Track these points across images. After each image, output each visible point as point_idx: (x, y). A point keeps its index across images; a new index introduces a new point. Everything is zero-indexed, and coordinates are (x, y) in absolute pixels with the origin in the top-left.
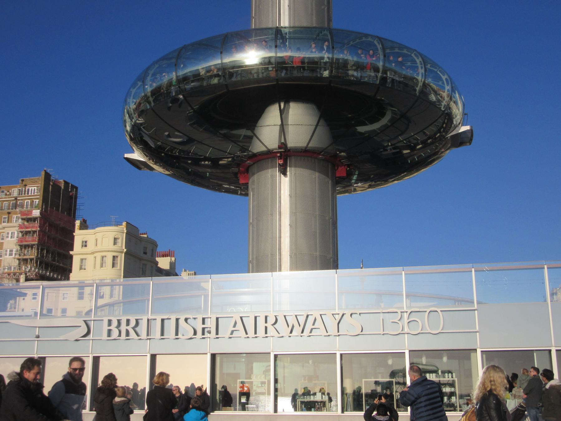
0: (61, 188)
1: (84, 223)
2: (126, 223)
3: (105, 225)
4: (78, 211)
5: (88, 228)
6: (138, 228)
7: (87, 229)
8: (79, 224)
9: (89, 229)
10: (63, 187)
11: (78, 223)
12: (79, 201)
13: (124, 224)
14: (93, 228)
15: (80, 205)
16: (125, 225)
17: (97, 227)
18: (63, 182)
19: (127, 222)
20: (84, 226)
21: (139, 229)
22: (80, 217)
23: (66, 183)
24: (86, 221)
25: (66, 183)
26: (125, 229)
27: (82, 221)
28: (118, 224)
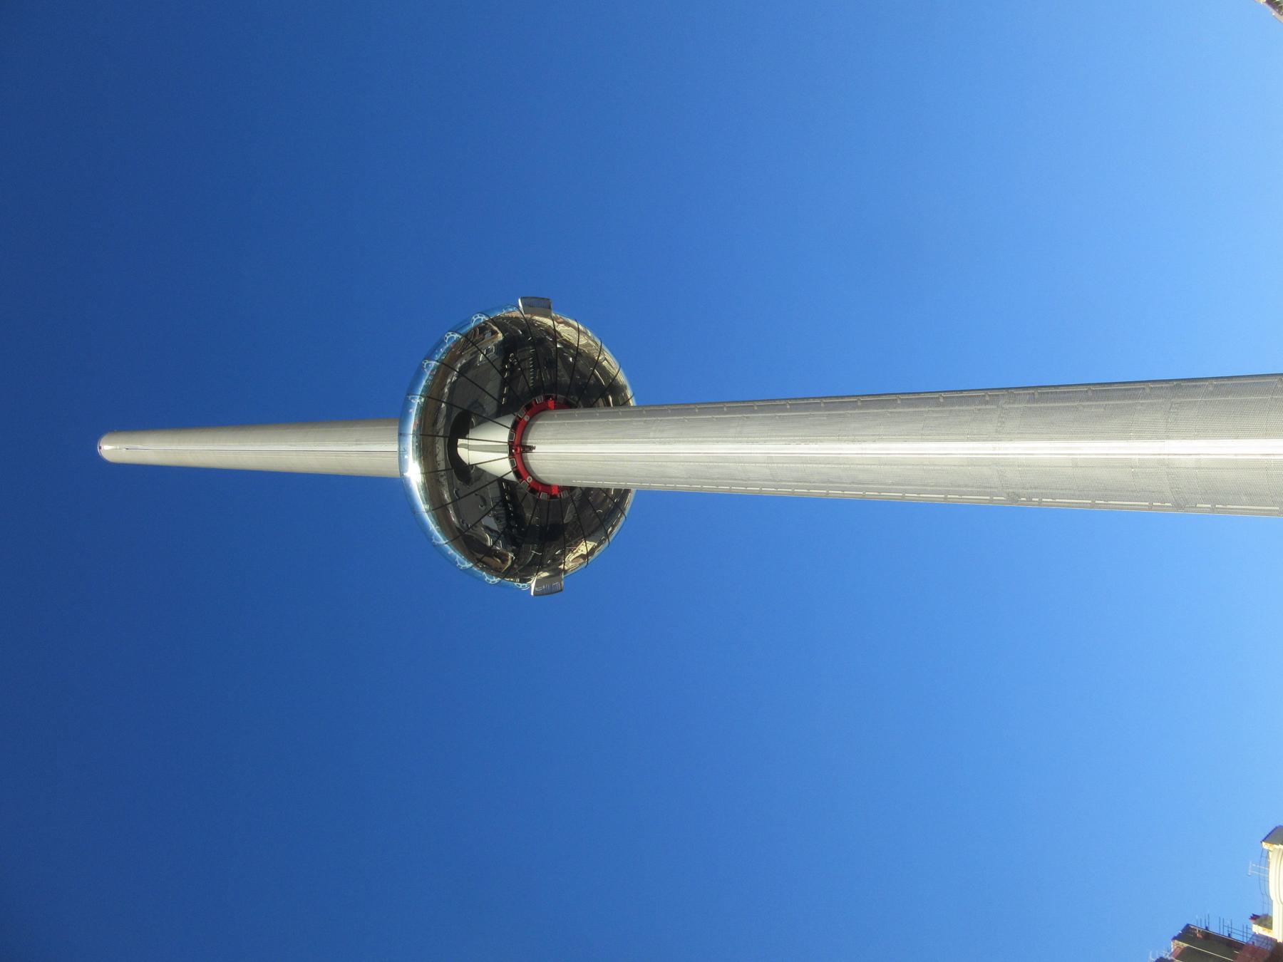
0: (1188, 947)
1: (1258, 920)
2: (1264, 843)
3: (1266, 881)
4: (1233, 931)
5: (1270, 914)
6: (1277, 827)
7: (1271, 918)
8: (1260, 927)
9: (1272, 914)
10: (1186, 945)
11: (1258, 929)
12: (1214, 929)
13: (1266, 846)
14: (1269, 903)
15: (1222, 926)
16: (1269, 845)
17: (1268, 896)
18: (1176, 941)
19: (1263, 841)
20: (1264, 920)
21: (1277, 825)
22: (1245, 930)
23: (1178, 938)
24: (1254, 915)
25: (1178, 938)
26: (1275, 846)
27: (1252, 921)
28: (1265, 856)
